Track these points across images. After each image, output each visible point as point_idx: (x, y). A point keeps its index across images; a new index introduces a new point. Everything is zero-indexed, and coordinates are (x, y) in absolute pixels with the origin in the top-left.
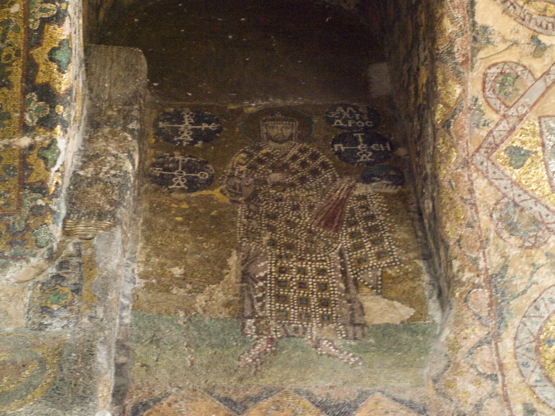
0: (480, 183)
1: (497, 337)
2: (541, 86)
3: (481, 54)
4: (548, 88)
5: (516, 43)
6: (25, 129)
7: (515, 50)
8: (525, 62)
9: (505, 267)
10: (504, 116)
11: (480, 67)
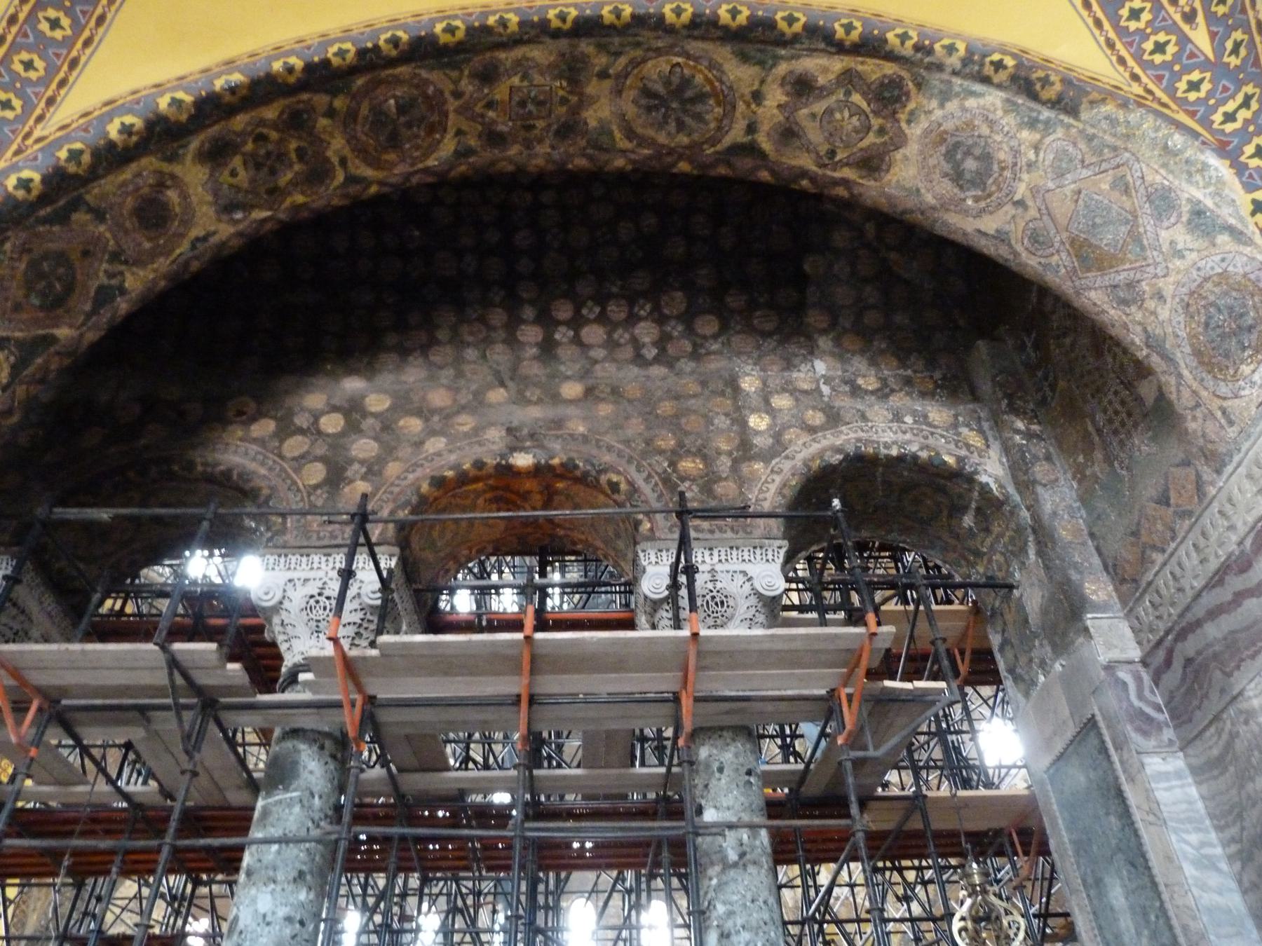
0: (1093, 294)
1: (1180, 376)
2: (1045, 218)
3: (1013, 242)
4: (1049, 214)
5: (1014, 217)
6: (970, 490)
7: (1018, 220)
8: (1028, 218)
9: (1145, 330)
10: (1058, 251)
11: (1019, 248)
